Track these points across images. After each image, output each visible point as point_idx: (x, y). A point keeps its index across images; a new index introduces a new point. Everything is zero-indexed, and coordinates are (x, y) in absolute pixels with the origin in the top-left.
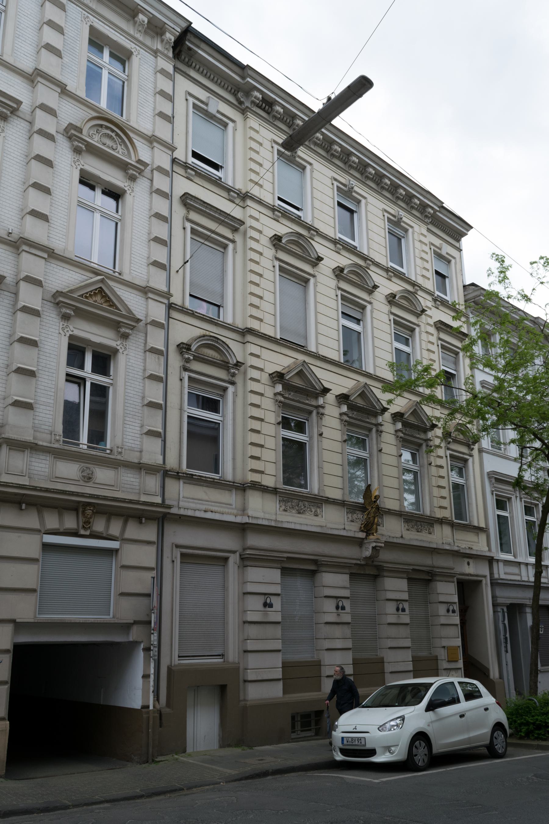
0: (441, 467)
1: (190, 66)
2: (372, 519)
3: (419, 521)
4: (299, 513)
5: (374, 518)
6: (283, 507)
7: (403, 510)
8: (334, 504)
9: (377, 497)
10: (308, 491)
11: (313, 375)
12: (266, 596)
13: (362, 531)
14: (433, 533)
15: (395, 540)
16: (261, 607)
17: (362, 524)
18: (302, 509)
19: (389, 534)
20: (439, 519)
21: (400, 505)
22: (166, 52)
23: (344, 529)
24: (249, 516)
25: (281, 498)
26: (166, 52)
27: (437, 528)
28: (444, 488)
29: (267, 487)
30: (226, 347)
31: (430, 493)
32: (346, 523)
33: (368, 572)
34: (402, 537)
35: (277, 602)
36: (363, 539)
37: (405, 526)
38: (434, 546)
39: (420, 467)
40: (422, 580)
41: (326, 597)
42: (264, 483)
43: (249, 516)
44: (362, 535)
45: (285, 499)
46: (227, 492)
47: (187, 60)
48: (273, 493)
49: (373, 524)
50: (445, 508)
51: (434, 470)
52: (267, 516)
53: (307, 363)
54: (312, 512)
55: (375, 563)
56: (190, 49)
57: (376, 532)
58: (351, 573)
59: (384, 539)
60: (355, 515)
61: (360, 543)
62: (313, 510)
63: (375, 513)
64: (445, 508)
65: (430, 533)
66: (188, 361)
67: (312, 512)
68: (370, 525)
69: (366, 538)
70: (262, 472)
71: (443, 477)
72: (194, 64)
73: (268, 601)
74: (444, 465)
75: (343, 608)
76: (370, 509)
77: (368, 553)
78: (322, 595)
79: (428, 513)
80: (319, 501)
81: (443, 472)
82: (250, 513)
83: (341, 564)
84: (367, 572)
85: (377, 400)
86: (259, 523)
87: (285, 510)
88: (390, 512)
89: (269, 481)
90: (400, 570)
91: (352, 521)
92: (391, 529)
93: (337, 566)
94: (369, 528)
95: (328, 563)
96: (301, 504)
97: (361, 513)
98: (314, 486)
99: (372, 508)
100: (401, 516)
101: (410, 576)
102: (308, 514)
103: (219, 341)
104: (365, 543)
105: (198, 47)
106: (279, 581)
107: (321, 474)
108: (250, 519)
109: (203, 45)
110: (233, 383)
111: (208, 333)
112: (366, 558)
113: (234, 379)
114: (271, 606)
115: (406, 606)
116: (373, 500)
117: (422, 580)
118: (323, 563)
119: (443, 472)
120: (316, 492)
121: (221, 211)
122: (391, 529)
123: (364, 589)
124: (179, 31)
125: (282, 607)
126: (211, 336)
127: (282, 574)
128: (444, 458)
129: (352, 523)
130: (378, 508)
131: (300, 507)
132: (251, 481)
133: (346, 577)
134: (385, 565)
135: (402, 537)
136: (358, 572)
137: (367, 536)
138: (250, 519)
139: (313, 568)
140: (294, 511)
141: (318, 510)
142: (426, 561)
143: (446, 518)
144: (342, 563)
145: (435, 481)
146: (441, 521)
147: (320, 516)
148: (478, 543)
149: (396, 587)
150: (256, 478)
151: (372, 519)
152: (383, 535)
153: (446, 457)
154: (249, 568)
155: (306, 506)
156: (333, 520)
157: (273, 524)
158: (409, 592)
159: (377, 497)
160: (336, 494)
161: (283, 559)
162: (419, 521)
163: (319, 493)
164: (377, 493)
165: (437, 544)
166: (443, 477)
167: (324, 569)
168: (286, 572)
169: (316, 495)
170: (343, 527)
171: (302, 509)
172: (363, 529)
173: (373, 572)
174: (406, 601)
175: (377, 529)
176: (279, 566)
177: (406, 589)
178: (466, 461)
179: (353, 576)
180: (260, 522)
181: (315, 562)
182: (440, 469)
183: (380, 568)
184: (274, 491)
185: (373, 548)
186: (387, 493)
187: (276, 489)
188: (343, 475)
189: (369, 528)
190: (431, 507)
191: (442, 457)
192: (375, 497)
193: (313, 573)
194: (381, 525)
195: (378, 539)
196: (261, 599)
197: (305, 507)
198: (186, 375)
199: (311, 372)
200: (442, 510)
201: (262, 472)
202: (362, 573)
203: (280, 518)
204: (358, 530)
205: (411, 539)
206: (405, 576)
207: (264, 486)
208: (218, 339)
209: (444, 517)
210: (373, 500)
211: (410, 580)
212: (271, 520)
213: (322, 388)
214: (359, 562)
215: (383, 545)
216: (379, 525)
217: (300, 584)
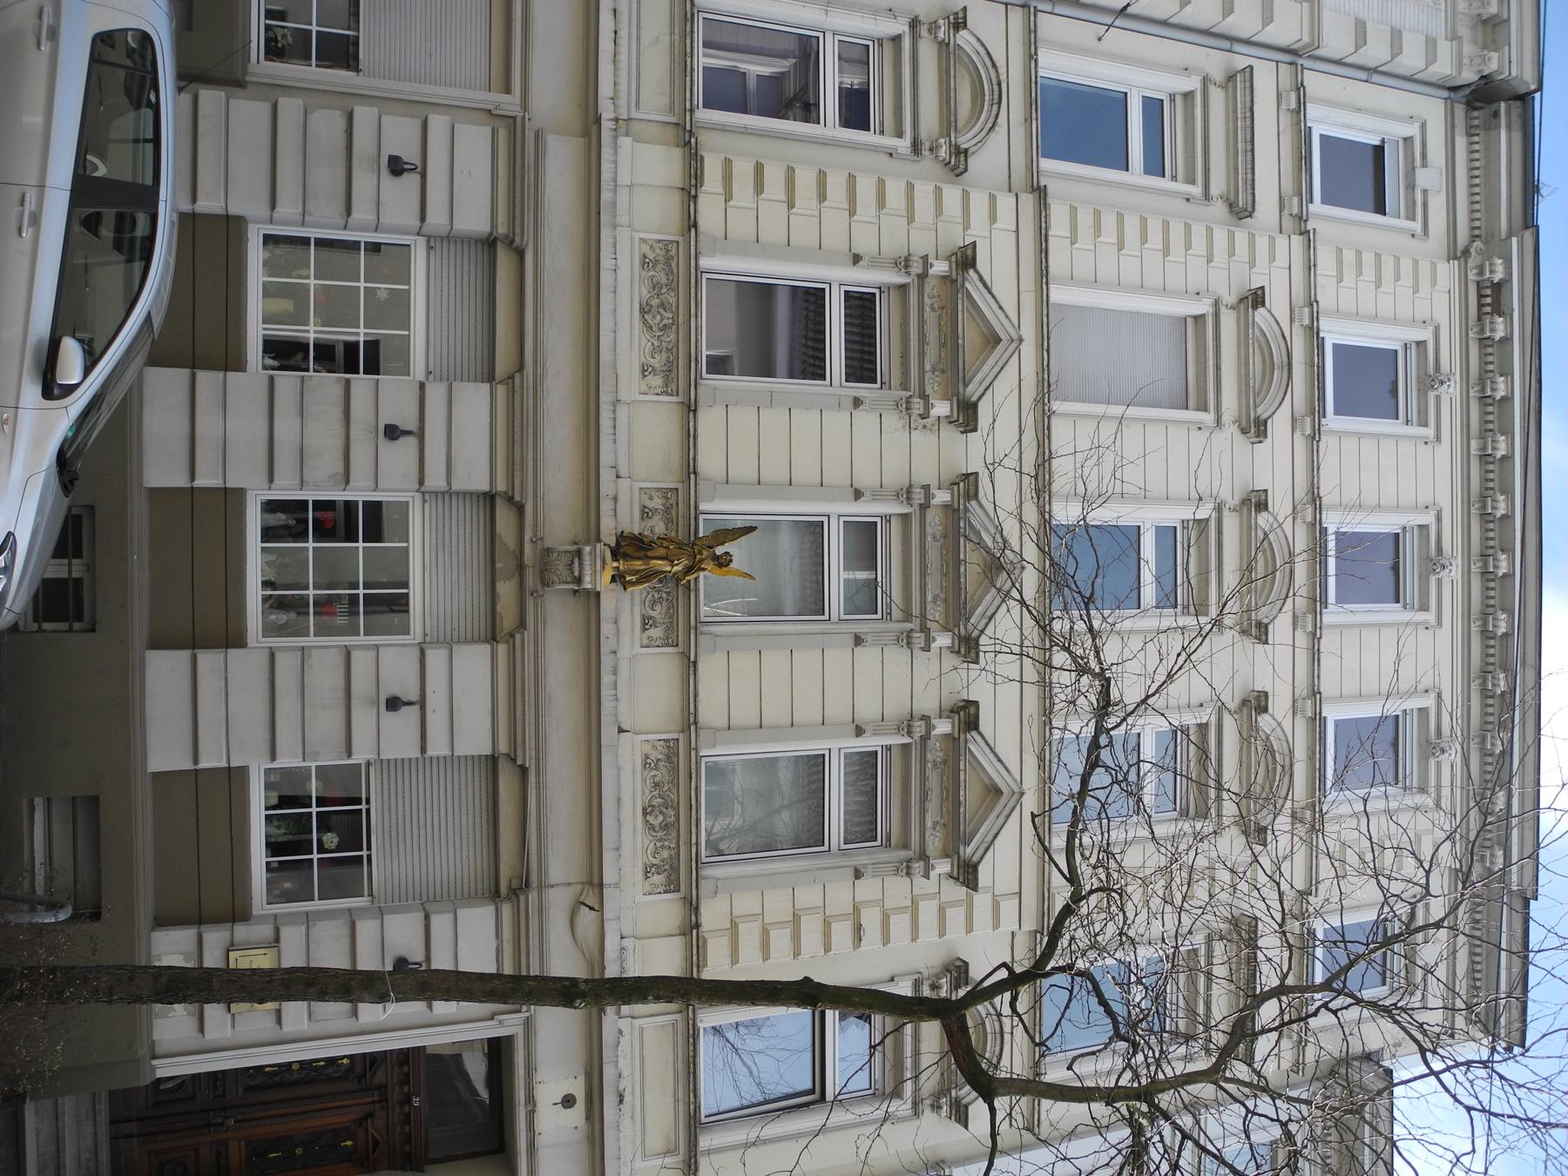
1: (1469, 135)
4: (643, 311)
11: (997, 369)
22: (1466, 61)
26: (1466, 61)
30: (989, 125)
46: (667, 100)
47: (1476, 122)
53: (1018, 349)
56: (1496, 114)
66: (933, 27)
68: (641, 554)
72: (1476, 139)
85: (989, 613)
87: (645, 262)
94: (629, 547)
103: (995, 107)
105: (1509, 129)
109: (1517, 136)
110: (916, 147)
111: (1002, 70)
113: (926, 153)
121: (1253, 150)
124: (1514, 74)
126: (999, 84)
148: (644, 1156)
151: (662, 552)
156: (640, 436)
159: (723, 562)
170: (622, 473)
173: (508, 620)
198: (900, 27)
199: (1000, 364)
202: (499, 565)
206: (503, 748)
208: (1000, 103)
211: (493, 761)
213: (974, 399)
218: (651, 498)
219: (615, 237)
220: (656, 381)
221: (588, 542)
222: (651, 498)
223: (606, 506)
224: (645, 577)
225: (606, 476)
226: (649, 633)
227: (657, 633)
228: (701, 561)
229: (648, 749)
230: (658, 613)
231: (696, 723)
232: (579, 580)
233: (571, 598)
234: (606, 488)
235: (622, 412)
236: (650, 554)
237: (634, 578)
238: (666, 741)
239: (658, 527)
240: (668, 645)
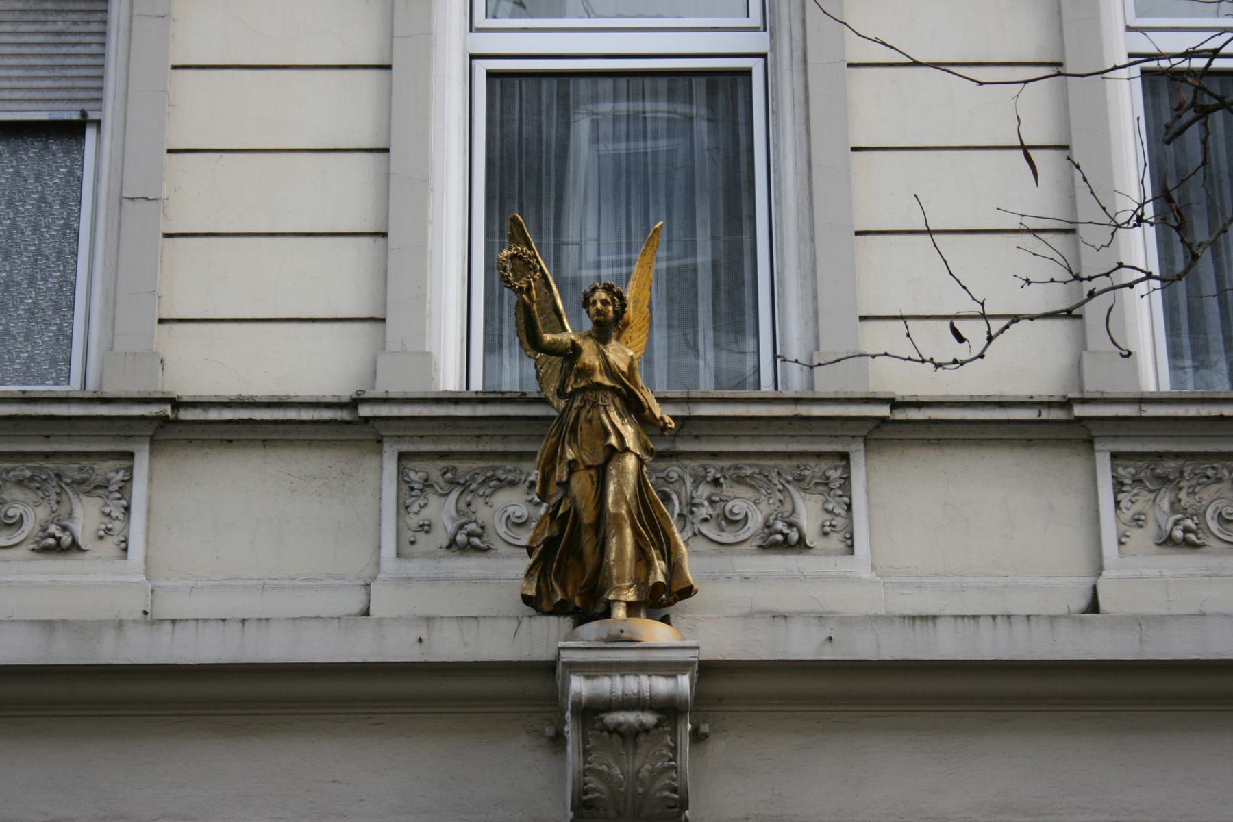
34: (1094, 607)
68: (588, 543)
94: (567, 574)
100: (1090, 442)
129: (470, 565)
151: (582, 484)
218: (426, 528)
220: (86, 516)
221: (553, 699)
222: (426, 528)
223: (449, 646)
224: (654, 535)
225: (361, 647)
226: (811, 537)
227: (809, 513)
228: (608, 369)
229: (1142, 538)
230: (754, 509)
231: (1067, 404)
232: (669, 709)
233: (717, 747)
234: (398, 647)
235: (169, 606)
236: (587, 517)
237: (660, 565)
238: (1119, 485)
239: (512, 508)
240: (847, 480)
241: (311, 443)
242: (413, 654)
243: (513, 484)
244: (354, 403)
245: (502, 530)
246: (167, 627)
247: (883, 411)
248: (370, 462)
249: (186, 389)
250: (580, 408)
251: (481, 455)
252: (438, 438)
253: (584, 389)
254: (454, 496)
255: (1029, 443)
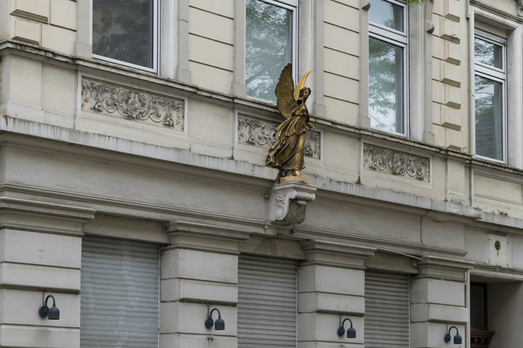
0: (454, 40)
2: (292, 139)
3: (398, 152)
4: (130, 117)
5: (298, 137)
6: (92, 103)
7: (363, 126)
8: (210, 103)
9: (305, 93)
10: (154, 70)
12: (46, 295)
13: (270, 165)
14: (426, 179)
15: (342, 189)
16: (34, 318)
17: (271, 150)
18: (136, 109)
19: (332, 175)
20: (441, 149)
21: (359, 116)
23: (232, 158)
24: (6, 117)
25: (88, 83)
27: (436, 168)
28: (457, 85)
29: (54, 54)
31: (427, 93)
32: (237, 146)
33: (281, 253)
34: (359, 182)
35: (70, 310)
36: (272, 182)
37: (366, 161)
38: (427, 205)
39: (409, 36)
40: (396, 273)
41: (183, 300)
42: (46, 45)
43: (6, 117)
44: (272, 174)
45: (97, 84)
48: (69, 70)
49: (294, 150)
50: (457, 128)
51: (437, 46)
52: (53, 120)
54: (159, 116)
55: (298, 235)
57: (301, 168)
58: (242, 254)
59: (319, 184)
60: (257, 130)
61: (266, 190)
62: (163, 114)
63: (299, 126)
64: (457, 128)
65: (421, 179)
67: (159, 116)
68: (288, 152)
69: (278, 181)
70: (43, 20)
71: (457, 63)
73: (50, 305)
74: (461, 34)
75: (220, 325)
76: (289, 120)
77: (280, 211)
78: (177, 298)
79: (418, 135)
80: (179, 95)
81: (457, 51)
82: (11, 110)
83: (221, 234)
84: (280, 253)
86: (31, 133)
87: (96, 110)
88: (334, 128)
89: (59, 43)
90: (350, 251)
91: (251, 143)
92: (335, 164)
93: (211, 236)
94: (284, 159)
95: (192, 230)
96: (134, 97)
97: (271, 126)
98: (168, 60)
99: (294, 115)
100: (359, 139)
101: (372, 266)
102: (149, 121)
104: (276, 192)
106: (79, 265)
107: (185, 33)
108: (11, 122)
112: (276, 223)
114: (54, 315)
115: (359, 325)
116: (297, 98)
117: (396, 273)
118: (180, 228)
119: (457, 51)
120: (170, 74)
122: (335, 164)
123: (271, 288)
125: (81, 320)
127: (85, 248)
128: (463, 20)
129: (251, 148)
130: (306, 117)
131: (133, 104)
132: (16, 38)
133: (233, 261)
134: (318, 239)
135: (359, 182)
136: (257, 252)
137: (280, 175)
138: (11, 122)
139: (158, 238)
140: (117, 113)
141: (174, 114)
142: (406, 236)
143: (456, 150)
144: (223, 230)
145: (438, 70)
146: (446, 155)
147: (177, 127)
149: (339, 286)
150: (29, 31)
151: (292, 139)
152: (316, 176)
153: (468, 19)
154: (7, 231)
155: (147, 103)
156: (209, 138)
157: (65, 137)
158: (369, 298)
160: (218, 83)
161: (87, 216)
162: (398, 152)
163: (177, 76)
164: (308, 84)
165: (432, 200)
166: (457, 63)
167: (182, 241)
168: (92, 243)
169: (168, 80)
170: (230, 155)
171: (136, 109)
172: (272, 160)
174: (360, 315)
175: (302, 161)
176: (79, 230)
177: (362, 292)
178: (509, 31)
179: (245, 258)
180: (33, 131)
181: (163, 226)
182: (452, 45)
183: (306, 245)
184: (72, 64)
185: (293, 201)
186: (333, 86)
187: (74, 59)
188: (234, 40)
189: (284, 159)
190: (425, 124)
191: (457, 19)
192: (302, 91)
193: (161, 249)
194: (315, 156)
195: (303, 183)
196: (36, 301)
197: (143, 105)
200: (448, 130)
201: (43, 20)
202: (269, 254)
203: (81, 126)
204: (263, 163)
205: (377, 189)
206: (360, 264)
207: (46, 51)
209: (451, 146)
210: (297, 98)
211: (370, 272)
212: (61, 128)
214: (261, 231)
215: (313, 196)
216: (310, 155)
217: (128, 274)
219: (94, 134)
241: (219, 105)
242: (249, 173)
243: (259, 126)
244: (233, 98)
245: (257, 139)
246: (208, 157)
247: (330, 124)
248: (231, 114)
249: (201, 86)
250: (299, 120)
251: (253, 117)
252: (246, 111)
253: (301, 116)
254: (248, 127)
255: (349, 136)
